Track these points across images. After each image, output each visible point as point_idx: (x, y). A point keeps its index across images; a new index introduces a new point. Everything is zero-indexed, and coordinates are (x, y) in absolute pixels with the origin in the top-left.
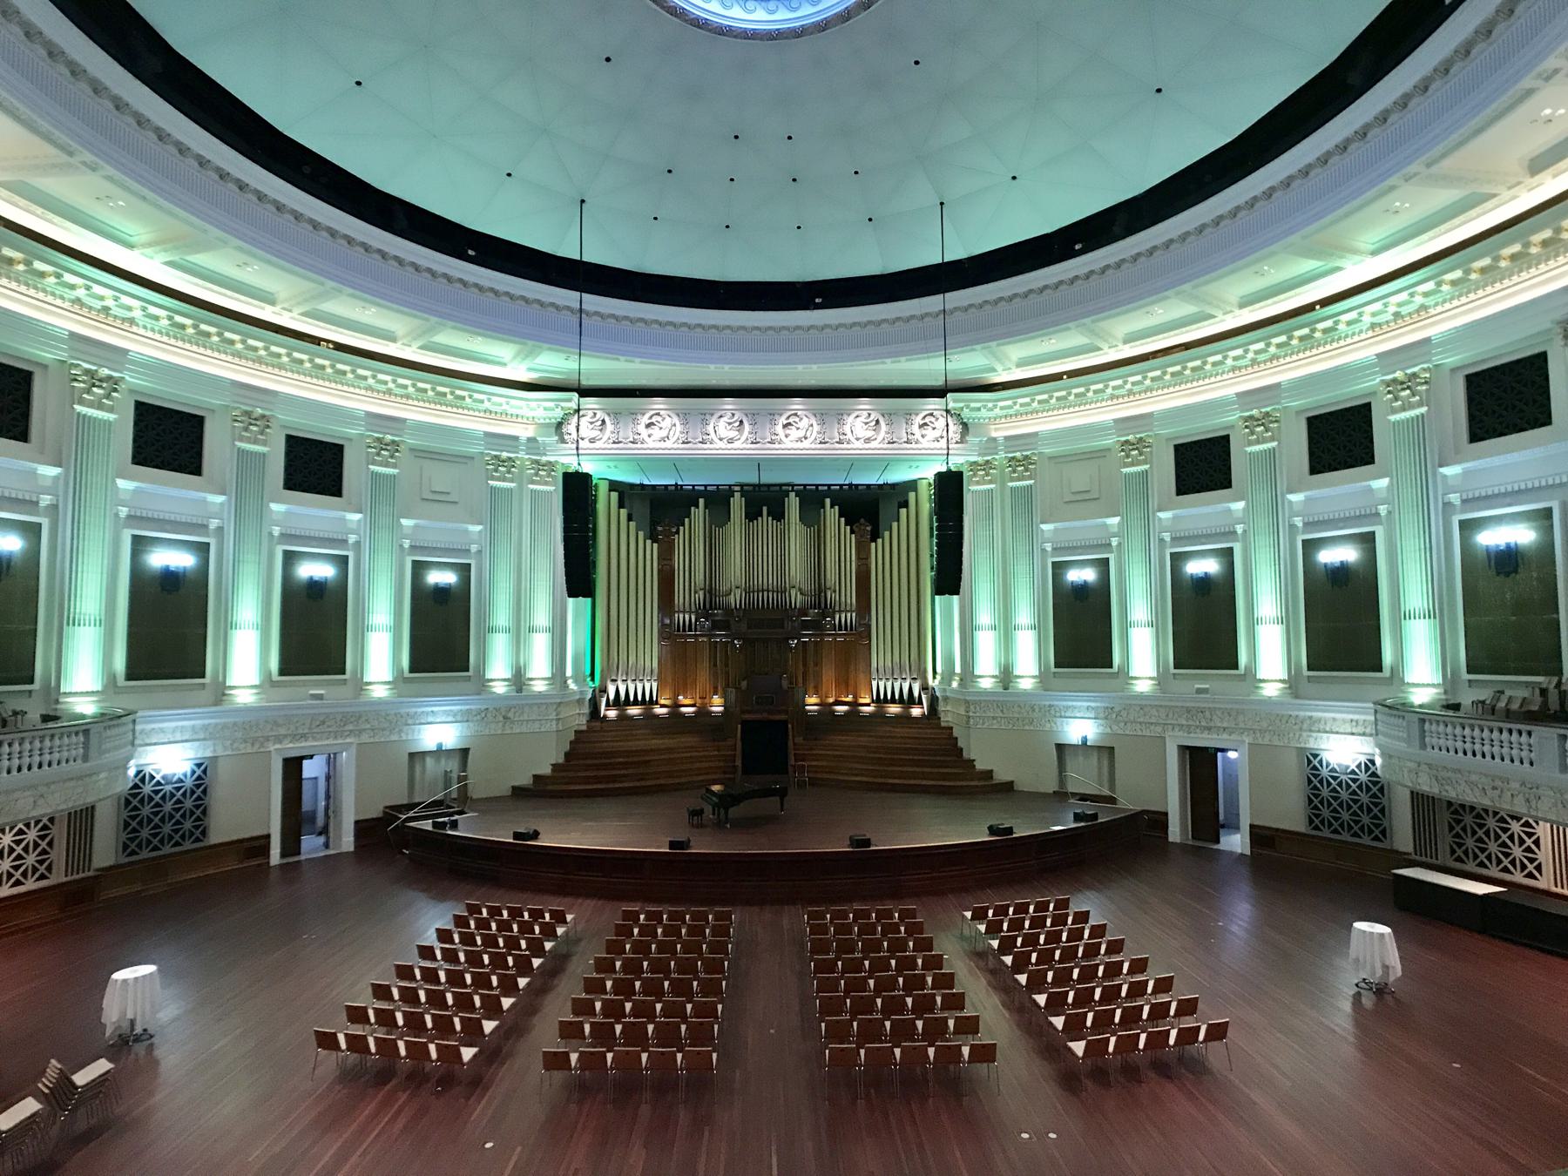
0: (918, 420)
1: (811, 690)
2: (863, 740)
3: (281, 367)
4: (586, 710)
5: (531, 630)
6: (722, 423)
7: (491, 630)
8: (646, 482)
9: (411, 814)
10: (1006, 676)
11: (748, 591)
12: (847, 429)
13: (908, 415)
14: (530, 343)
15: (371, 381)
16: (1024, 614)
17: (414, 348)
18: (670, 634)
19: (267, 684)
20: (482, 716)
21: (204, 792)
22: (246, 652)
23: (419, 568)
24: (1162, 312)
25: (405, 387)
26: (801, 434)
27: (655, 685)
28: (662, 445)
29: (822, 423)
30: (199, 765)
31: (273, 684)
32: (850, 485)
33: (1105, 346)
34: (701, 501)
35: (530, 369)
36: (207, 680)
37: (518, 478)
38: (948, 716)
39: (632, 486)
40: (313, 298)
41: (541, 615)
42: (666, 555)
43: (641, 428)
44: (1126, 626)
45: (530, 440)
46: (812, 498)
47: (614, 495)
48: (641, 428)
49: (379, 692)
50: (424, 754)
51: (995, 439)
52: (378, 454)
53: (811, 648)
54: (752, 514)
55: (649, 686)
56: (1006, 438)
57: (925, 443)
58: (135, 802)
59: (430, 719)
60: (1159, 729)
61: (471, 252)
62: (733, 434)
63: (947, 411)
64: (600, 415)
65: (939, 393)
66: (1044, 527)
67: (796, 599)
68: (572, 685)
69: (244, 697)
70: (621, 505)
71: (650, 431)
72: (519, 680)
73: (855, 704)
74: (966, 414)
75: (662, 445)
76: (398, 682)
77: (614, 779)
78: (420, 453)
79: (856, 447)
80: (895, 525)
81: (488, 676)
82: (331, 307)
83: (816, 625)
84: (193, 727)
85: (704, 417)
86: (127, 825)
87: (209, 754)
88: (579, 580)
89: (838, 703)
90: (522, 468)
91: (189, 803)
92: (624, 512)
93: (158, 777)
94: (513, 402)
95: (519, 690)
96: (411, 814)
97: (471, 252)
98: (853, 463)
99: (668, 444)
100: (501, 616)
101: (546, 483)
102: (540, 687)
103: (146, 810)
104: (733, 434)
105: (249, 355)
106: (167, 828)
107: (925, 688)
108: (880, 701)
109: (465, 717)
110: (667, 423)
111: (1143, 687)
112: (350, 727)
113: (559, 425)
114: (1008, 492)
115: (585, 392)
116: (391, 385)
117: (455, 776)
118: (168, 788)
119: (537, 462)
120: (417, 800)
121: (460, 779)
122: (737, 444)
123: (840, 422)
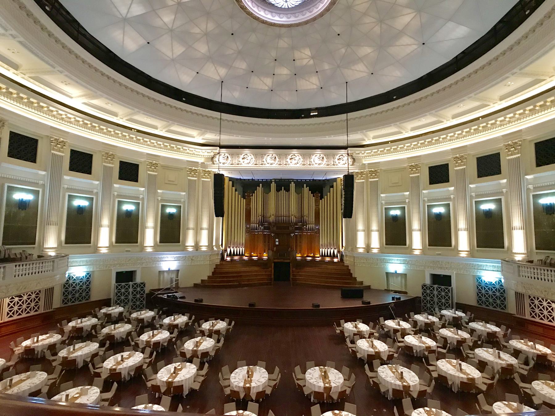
0: (337, 157)
1: (298, 252)
2: (316, 270)
3: (119, 138)
4: (220, 257)
5: (202, 229)
6: (269, 158)
7: (188, 229)
8: (242, 178)
9: (159, 292)
10: (368, 248)
11: (277, 216)
12: (312, 160)
13: (334, 156)
14: (203, 130)
15: (149, 143)
16: (374, 226)
17: (164, 130)
18: (249, 231)
19: (111, 247)
20: (184, 259)
21: (90, 283)
22: (104, 236)
23: (163, 207)
24: (424, 121)
25: (160, 145)
26: (296, 162)
27: (243, 249)
28: (248, 165)
29: (304, 158)
30: (88, 274)
31: (113, 246)
32: (313, 180)
33: (404, 132)
34: (261, 185)
35: (203, 139)
36: (91, 244)
37: (199, 177)
38: (347, 261)
39: (237, 179)
40: (130, 114)
41: (205, 225)
42: (248, 204)
43: (241, 159)
44: (411, 230)
45: (202, 163)
46: (299, 184)
47: (231, 182)
48: (241, 159)
49: (149, 250)
50: (164, 271)
51: (365, 164)
52: (151, 168)
53: (299, 236)
54: (278, 189)
55: (242, 249)
56: (369, 164)
58: (67, 286)
59: (166, 259)
60: (423, 268)
61: (184, 99)
62: (272, 162)
63: (348, 154)
64: (227, 155)
65: (345, 148)
66: (382, 195)
67: (294, 219)
68: (215, 249)
69: (104, 251)
70: (233, 186)
71: (243, 160)
72: (197, 246)
73: (314, 257)
74: (354, 155)
75: (248, 165)
76: (155, 247)
77: (230, 281)
78: (165, 167)
79: (315, 167)
80: (329, 194)
81: (187, 245)
82: (136, 117)
83: (300, 229)
84: (87, 261)
85: (262, 156)
86: (64, 293)
87: (91, 270)
88: (219, 212)
89: (308, 256)
90: (199, 173)
91: (84, 287)
92: (234, 188)
93: (75, 278)
94: (196, 150)
95: (197, 250)
96: (159, 292)
97: (184, 99)
98: (314, 172)
99: (250, 165)
100: (191, 225)
101: (208, 178)
102: (204, 249)
103: (70, 289)
104: (272, 162)
105: (108, 133)
106: (77, 295)
107: (339, 252)
108: (323, 256)
109: (178, 259)
110: (249, 158)
111: (417, 252)
112: (139, 261)
113: (212, 158)
114: (369, 183)
115: (221, 147)
116: (155, 144)
117: (174, 279)
118: (78, 281)
119: (204, 171)
120: (161, 288)
121: (176, 280)
122: (273, 165)
123: (310, 158)
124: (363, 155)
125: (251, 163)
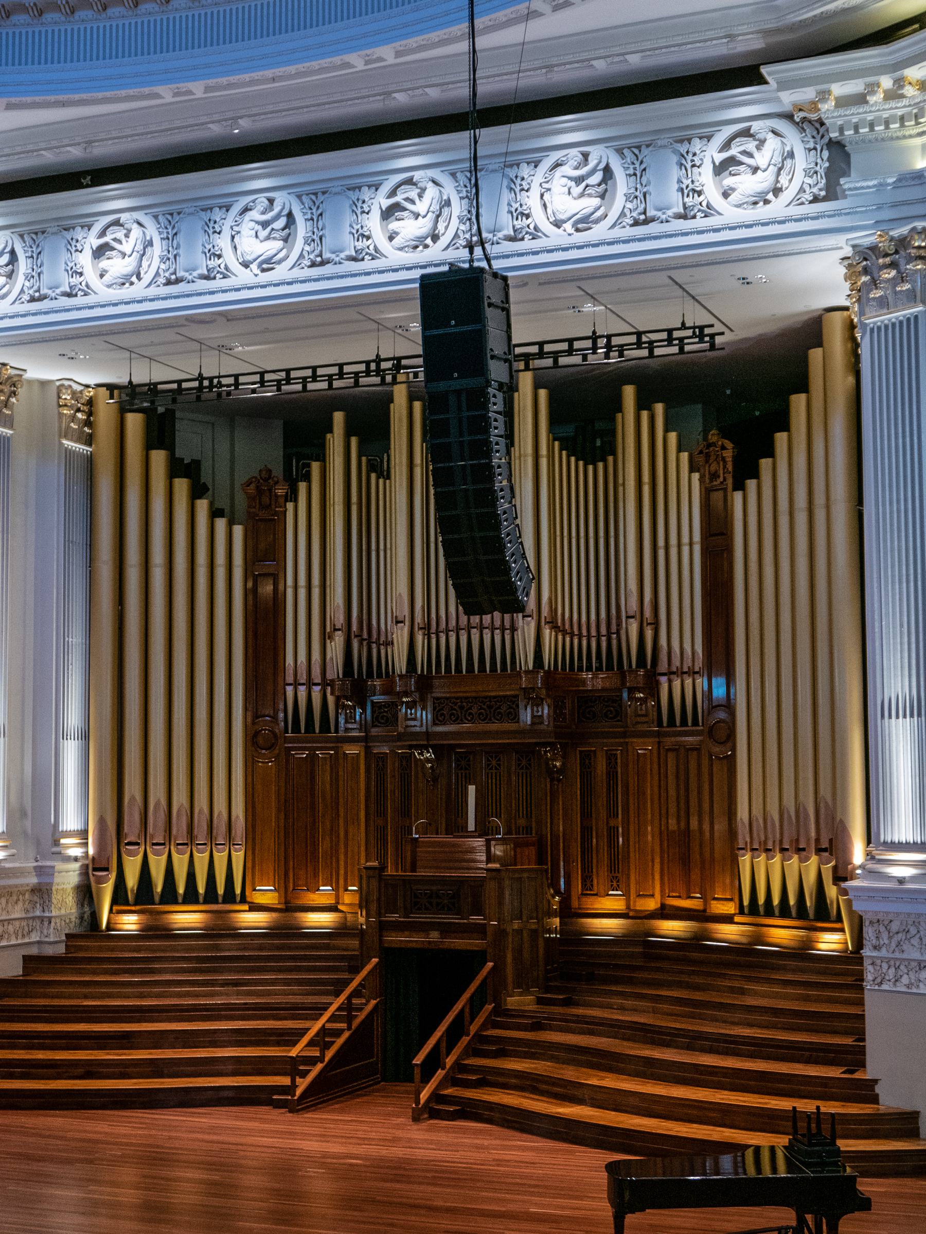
12: (532, 201)
57: (728, 212)
63: (789, 117)
123: (515, 186)
124: (899, 108)
125: (147, 278)
